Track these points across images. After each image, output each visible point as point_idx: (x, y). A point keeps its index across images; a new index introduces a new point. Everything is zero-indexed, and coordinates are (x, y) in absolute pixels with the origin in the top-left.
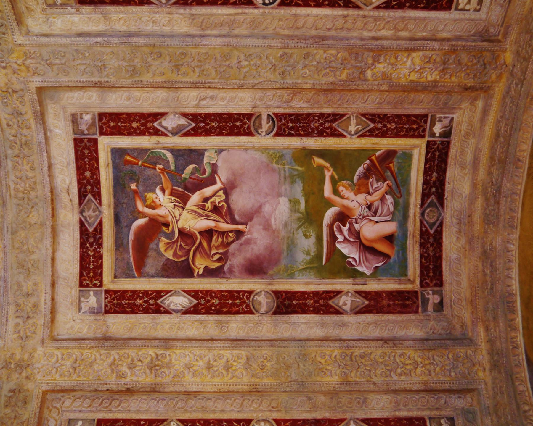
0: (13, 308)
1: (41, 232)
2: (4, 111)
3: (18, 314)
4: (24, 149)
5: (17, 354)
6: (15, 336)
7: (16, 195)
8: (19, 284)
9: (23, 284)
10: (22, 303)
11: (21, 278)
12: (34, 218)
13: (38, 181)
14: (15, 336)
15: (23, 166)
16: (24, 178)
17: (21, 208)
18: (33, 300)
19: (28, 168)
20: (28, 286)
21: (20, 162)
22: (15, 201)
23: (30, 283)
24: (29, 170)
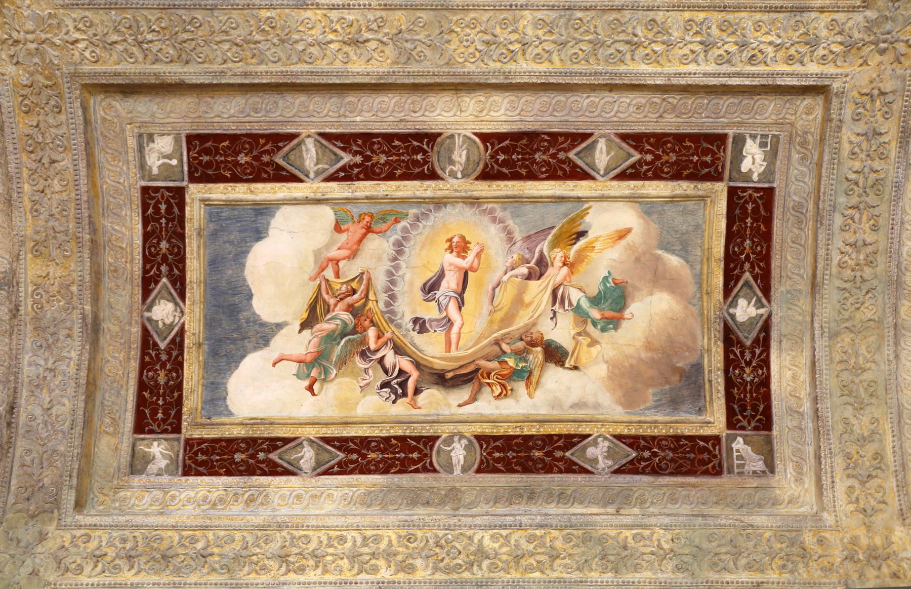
0: (840, 461)
1: (878, 335)
2: (852, 130)
3: (849, 471)
4: (868, 195)
5: (862, 537)
6: (852, 507)
7: (839, 273)
8: (846, 422)
9: (854, 421)
10: (854, 452)
11: (849, 412)
12: (868, 312)
13: (880, 249)
14: (852, 507)
15: (860, 224)
16: (860, 243)
17: (847, 295)
18: (871, 448)
19: (867, 227)
20: (862, 425)
21: (857, 216)
22: (838, 283)
23: (865, 420)
24: (868, 230)
